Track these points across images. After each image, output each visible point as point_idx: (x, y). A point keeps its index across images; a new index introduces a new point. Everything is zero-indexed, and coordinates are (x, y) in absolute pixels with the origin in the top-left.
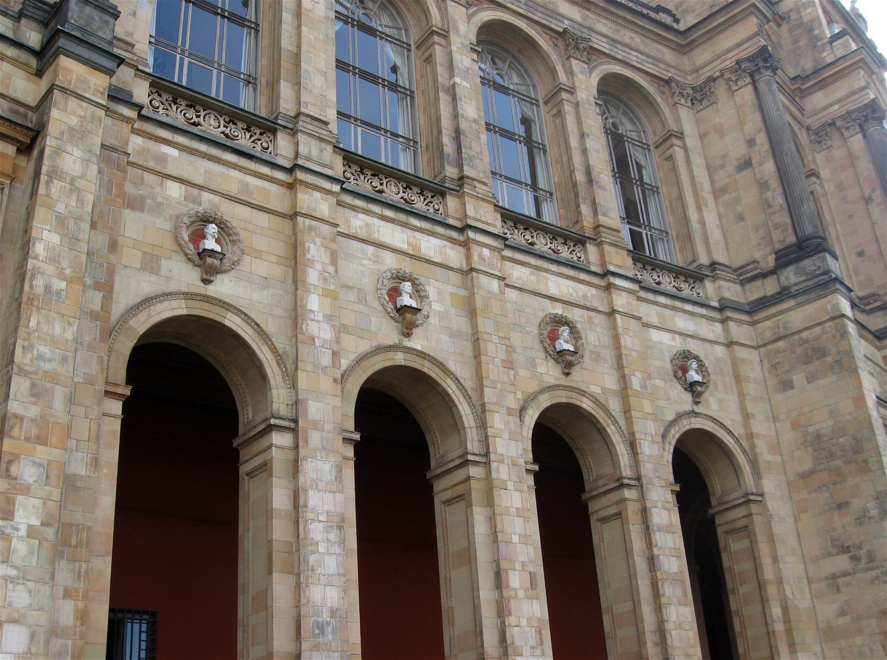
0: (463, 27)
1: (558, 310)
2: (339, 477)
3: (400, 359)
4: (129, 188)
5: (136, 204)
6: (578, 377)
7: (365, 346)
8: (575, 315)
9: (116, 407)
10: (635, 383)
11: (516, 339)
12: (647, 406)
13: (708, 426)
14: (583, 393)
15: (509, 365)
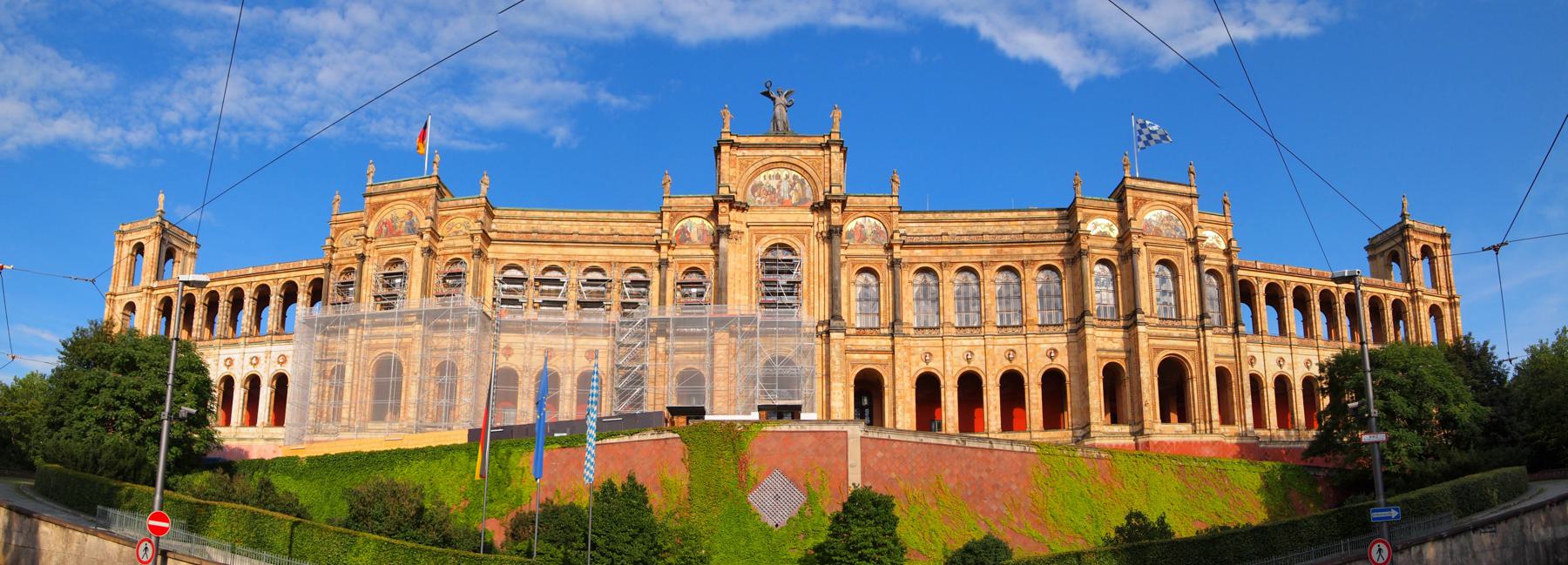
0: (988, 277)
1: (1011, 347)
2: (953, 394)
3: (968, 369)
4: (912, 352)
5: (913, 354)
6: (1014, 362)
7: (959, 368)
8: (1015, 348)
9: (914, 390)
10: (1031, 361)
11: (997, 357)
12: (1034, 366)
13: (1056, 366)
14: (1014, 366)
15: (994, 364)
